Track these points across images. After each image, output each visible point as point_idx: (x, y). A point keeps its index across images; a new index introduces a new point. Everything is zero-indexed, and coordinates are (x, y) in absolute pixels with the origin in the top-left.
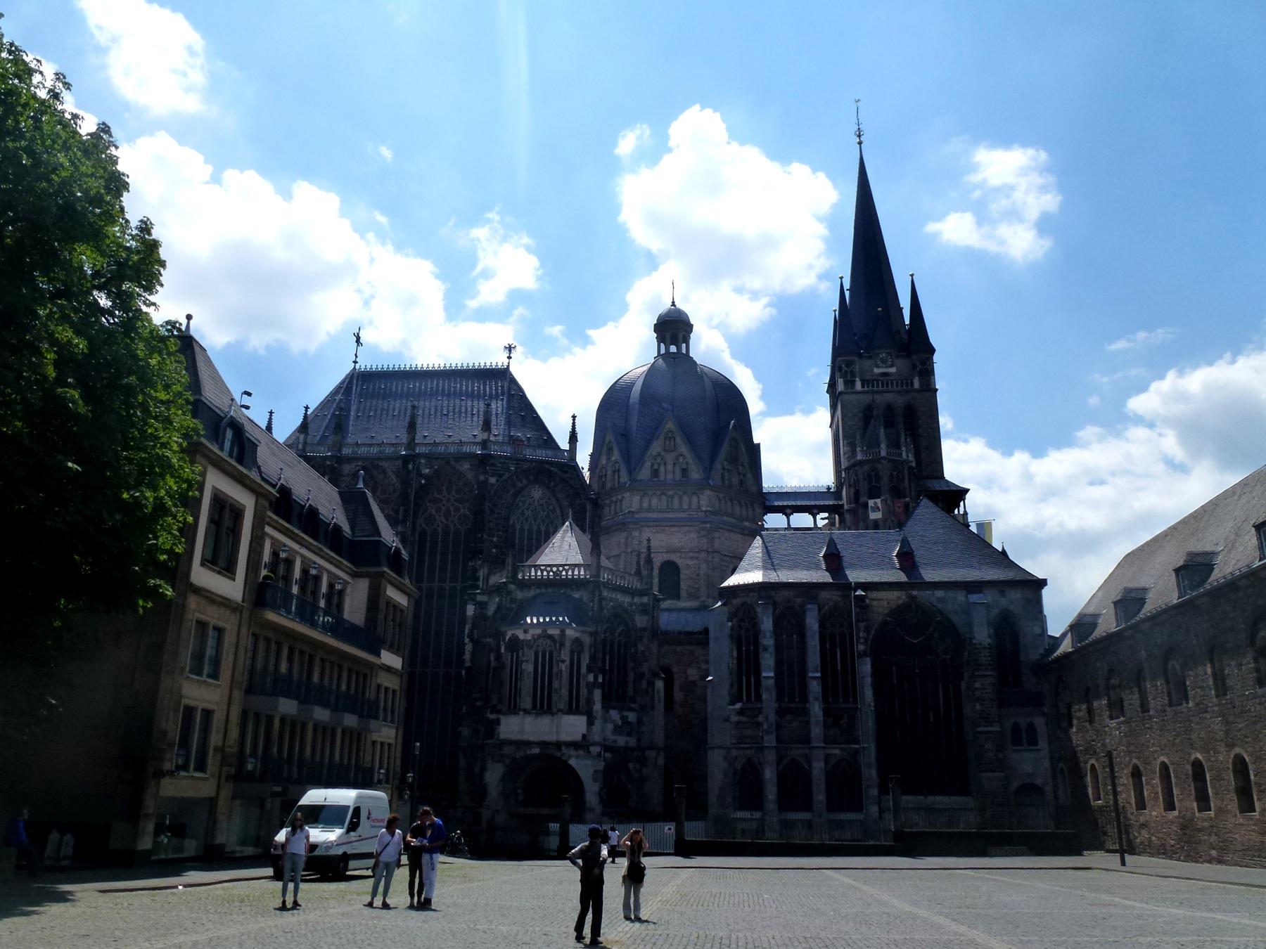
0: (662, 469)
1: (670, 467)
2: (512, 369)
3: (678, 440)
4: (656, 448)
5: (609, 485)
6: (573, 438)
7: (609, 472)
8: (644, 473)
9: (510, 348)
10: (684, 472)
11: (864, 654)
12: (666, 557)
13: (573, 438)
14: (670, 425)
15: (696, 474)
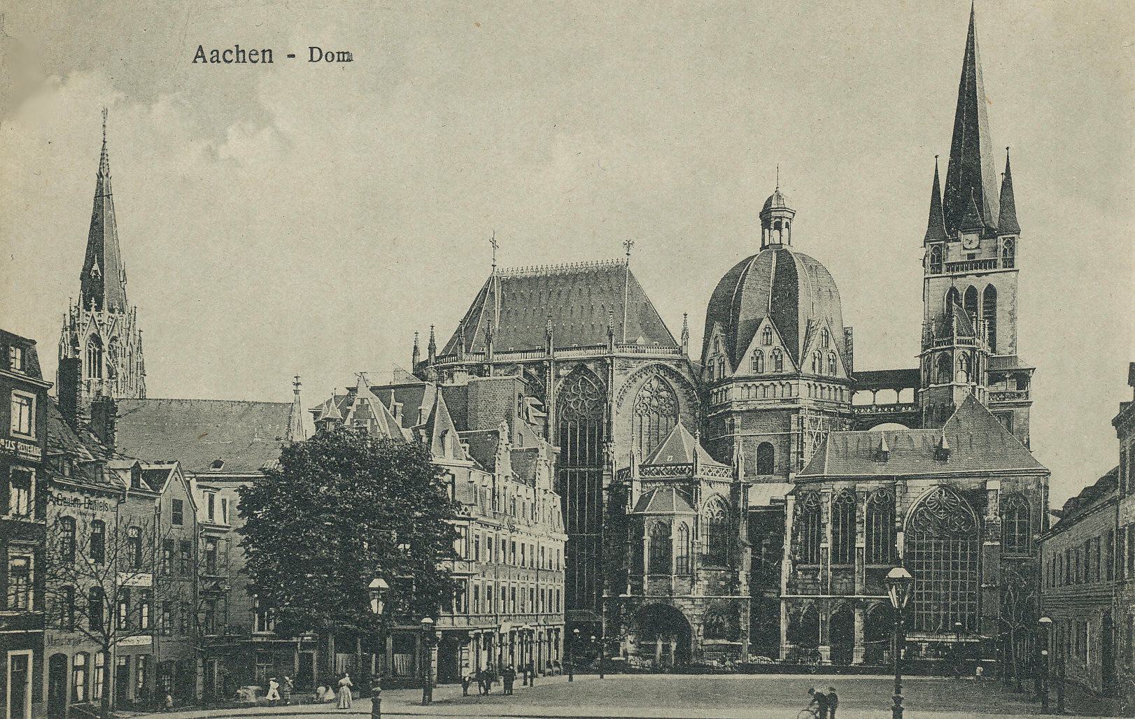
0: (760, 361)
1: (767, 360)
2: (632, 268)
3: (775, 335)
4: (756, 342)
5: (716, 377)
6: (685, 333)
7: (717, 365)
8: (745, 368)
9: (629, 245)
10: (779, 364)
11: (900, 530)
12: (765, 440)
13: (685, 333)
14: (766, 322)
15: (788, 368)
